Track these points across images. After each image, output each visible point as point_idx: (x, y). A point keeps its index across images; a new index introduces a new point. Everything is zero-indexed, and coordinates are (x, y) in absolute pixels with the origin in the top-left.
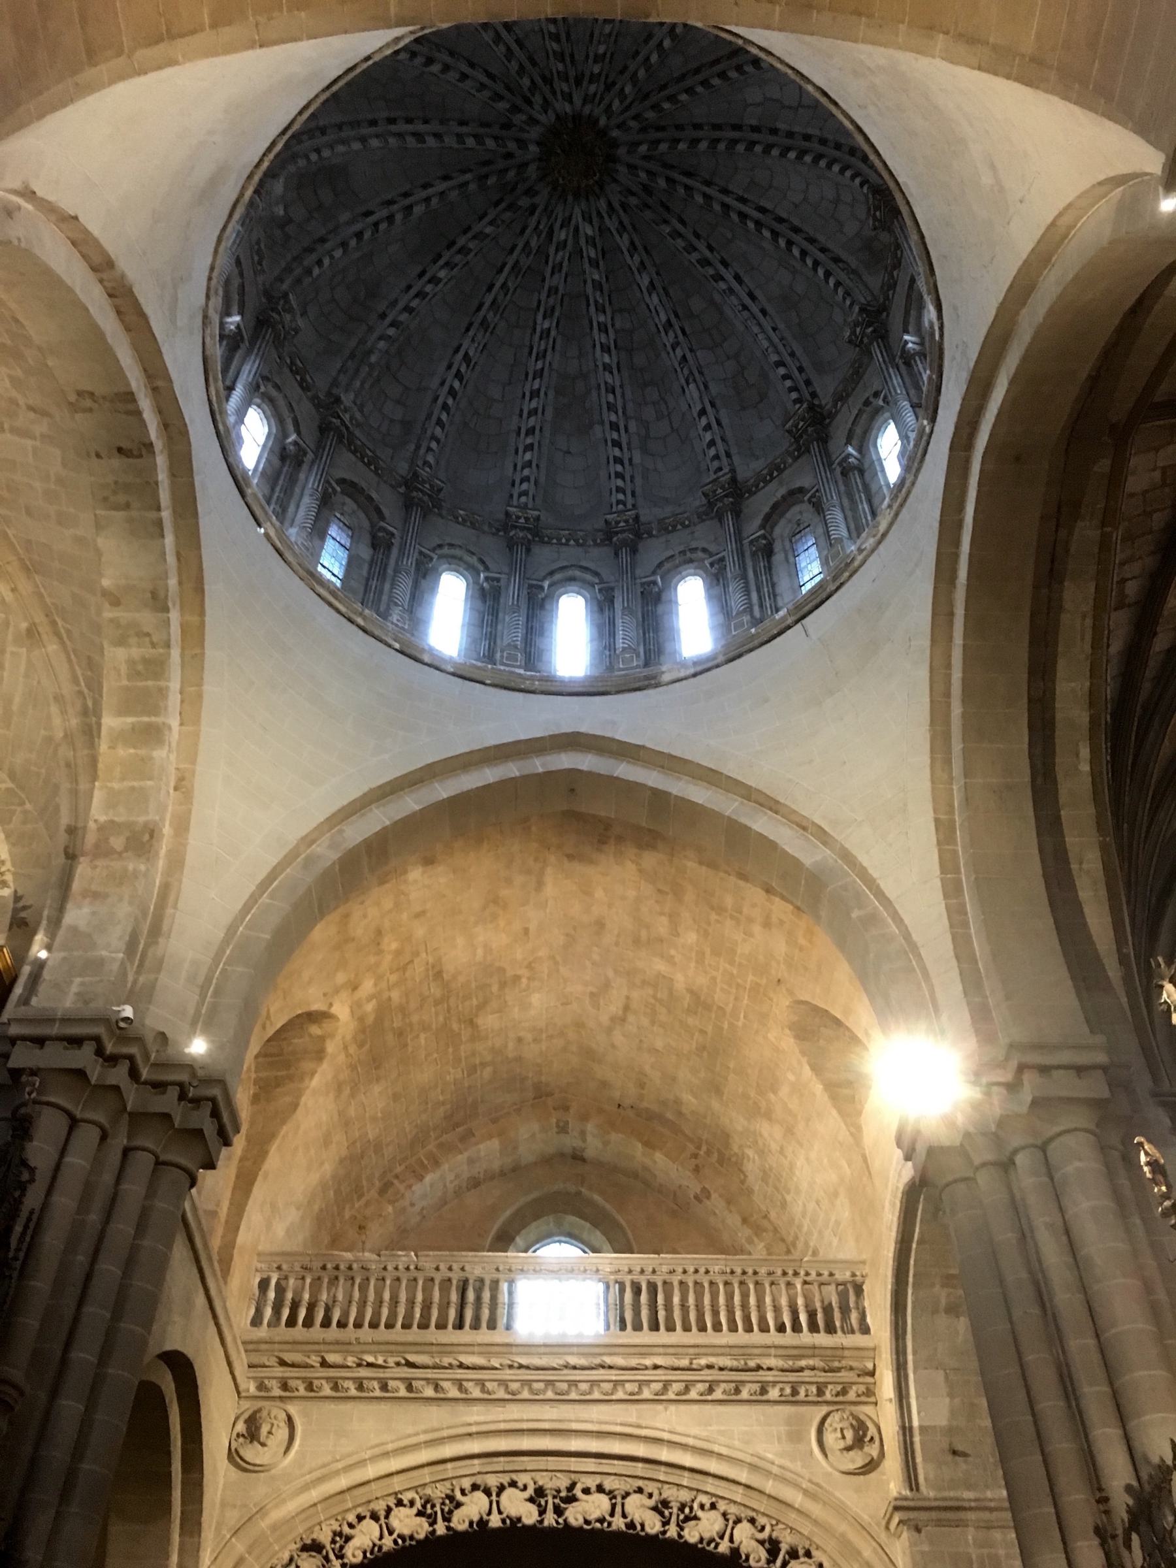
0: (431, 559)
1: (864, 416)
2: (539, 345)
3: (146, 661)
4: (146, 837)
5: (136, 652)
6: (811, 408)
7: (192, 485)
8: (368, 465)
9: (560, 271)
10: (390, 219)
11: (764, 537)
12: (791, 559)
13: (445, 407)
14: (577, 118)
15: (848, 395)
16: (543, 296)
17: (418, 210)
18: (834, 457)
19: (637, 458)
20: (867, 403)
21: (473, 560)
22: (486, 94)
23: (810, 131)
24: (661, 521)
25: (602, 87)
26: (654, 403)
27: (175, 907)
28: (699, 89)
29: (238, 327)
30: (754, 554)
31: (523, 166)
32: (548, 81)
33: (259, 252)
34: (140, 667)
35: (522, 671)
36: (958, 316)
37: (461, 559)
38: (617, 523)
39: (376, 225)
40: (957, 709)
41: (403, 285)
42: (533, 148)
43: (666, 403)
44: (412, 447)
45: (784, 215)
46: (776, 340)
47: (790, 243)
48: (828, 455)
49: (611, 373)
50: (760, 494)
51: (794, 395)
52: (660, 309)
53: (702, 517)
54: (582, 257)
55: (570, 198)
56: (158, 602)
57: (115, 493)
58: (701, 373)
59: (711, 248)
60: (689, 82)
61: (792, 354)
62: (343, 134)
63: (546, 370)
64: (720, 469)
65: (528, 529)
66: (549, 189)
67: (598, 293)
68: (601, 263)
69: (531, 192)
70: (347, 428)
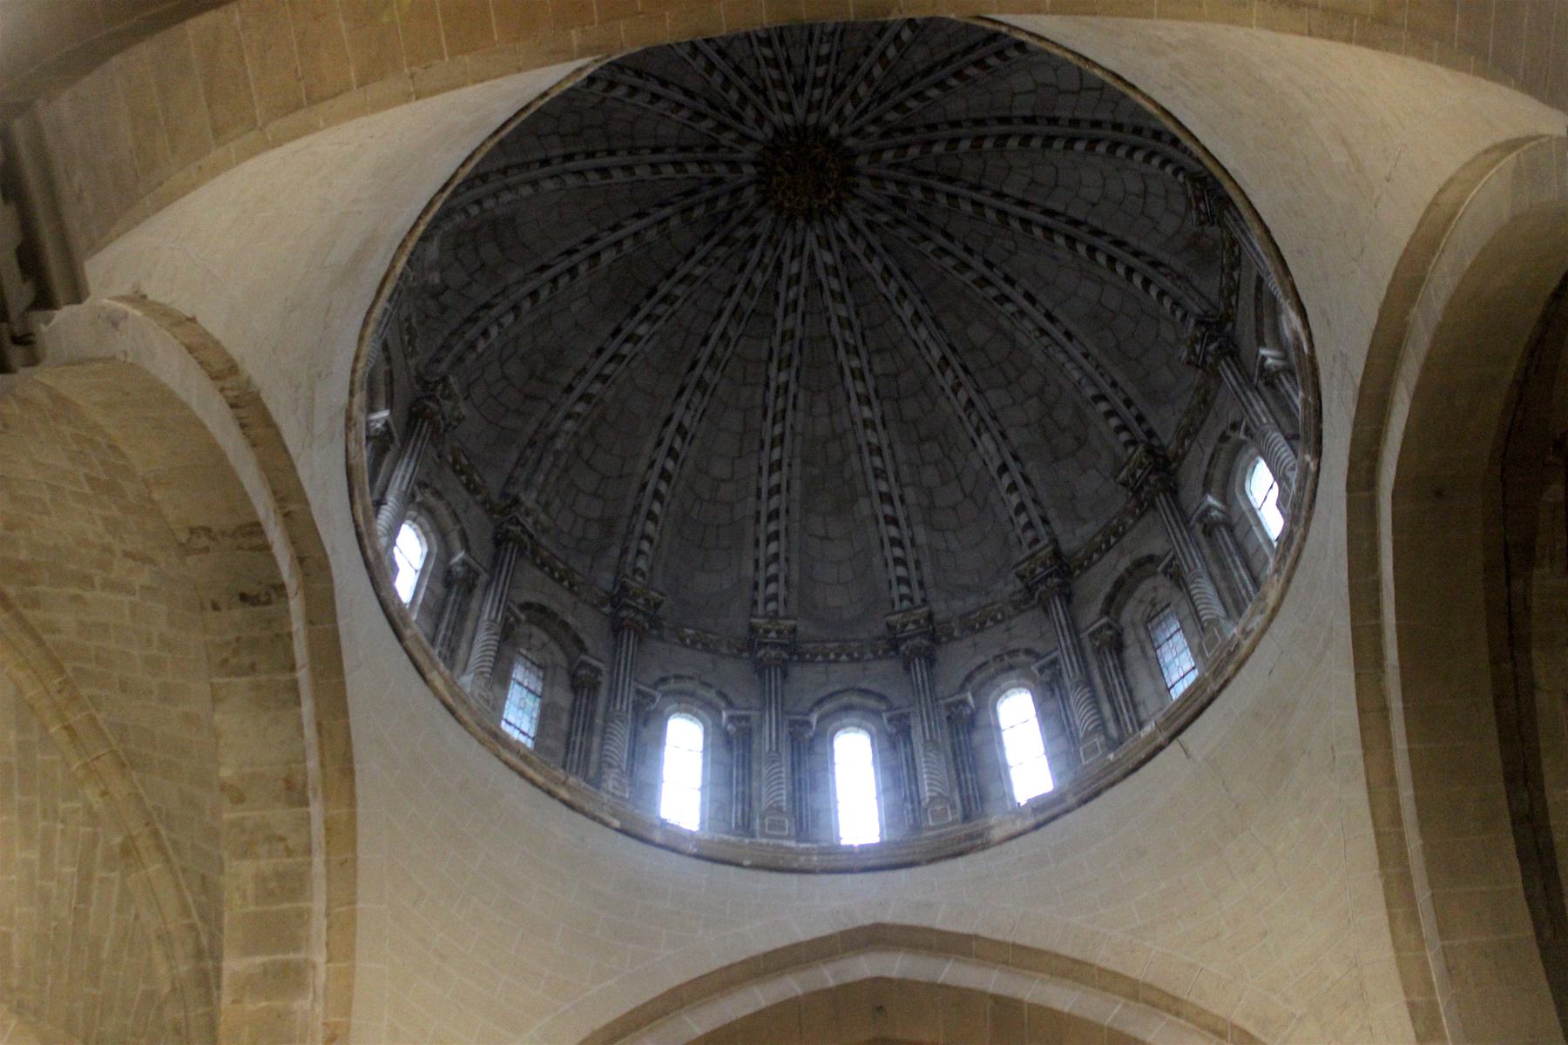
0: (653, 699)
1: (1223, 455)
2: (775, 405)
3: (281, 876)
5: (266, 865)
6: (1150, 451)
7: (336, 630)
8: (561, 580)
9: (795, 310)
10: (572, 271)
11: (1109, 627)
12: (1151, 653)
13: (657, 495)
14: (801, 130)
15: (1197, 432)
16: (776, 340)
17: (607, 257)
18: (1190, 511)
19: (922, 536)
20: (1224, 438)
21: (711, 694)
22: (685, 113)
23: (1099, 116)
24: (964, 617)
25: (829, 91)
28: (953, 82)
29: (386, 424)
30: (1098, 651)
31: (736, 191)
32: (763, 92)
33: (410, 330)
34: (272, 885)
35: (792, 844)
37: (693, 695)
38: (904, 625)
39: (554, 280)
40: (1414, 842)
41: (592, 349)
42: (749, 170)
44: (615, 551)
45: (1081, 216)
46: (1089, 368)
47: (1092, 250)
48: (1182, 512)
49: (875, 430)
50: (1094, 570)
51: (1124, 436)
52: (931, 344)
53: (1020, 606)
54: (822, 291)
55: (800, 224)
56: (294, 792)
57: (236, 652)
58: (995, 418)
60: (940, 74)
61: (1114, 384)
62: (510, 180)
63: (788, 432)
64: (1036, 541)
65: (782, 646)
66: (773, 215)
67: (847, 333)
68: (848, 296)
69: (748, 221)
70: (531, 536)
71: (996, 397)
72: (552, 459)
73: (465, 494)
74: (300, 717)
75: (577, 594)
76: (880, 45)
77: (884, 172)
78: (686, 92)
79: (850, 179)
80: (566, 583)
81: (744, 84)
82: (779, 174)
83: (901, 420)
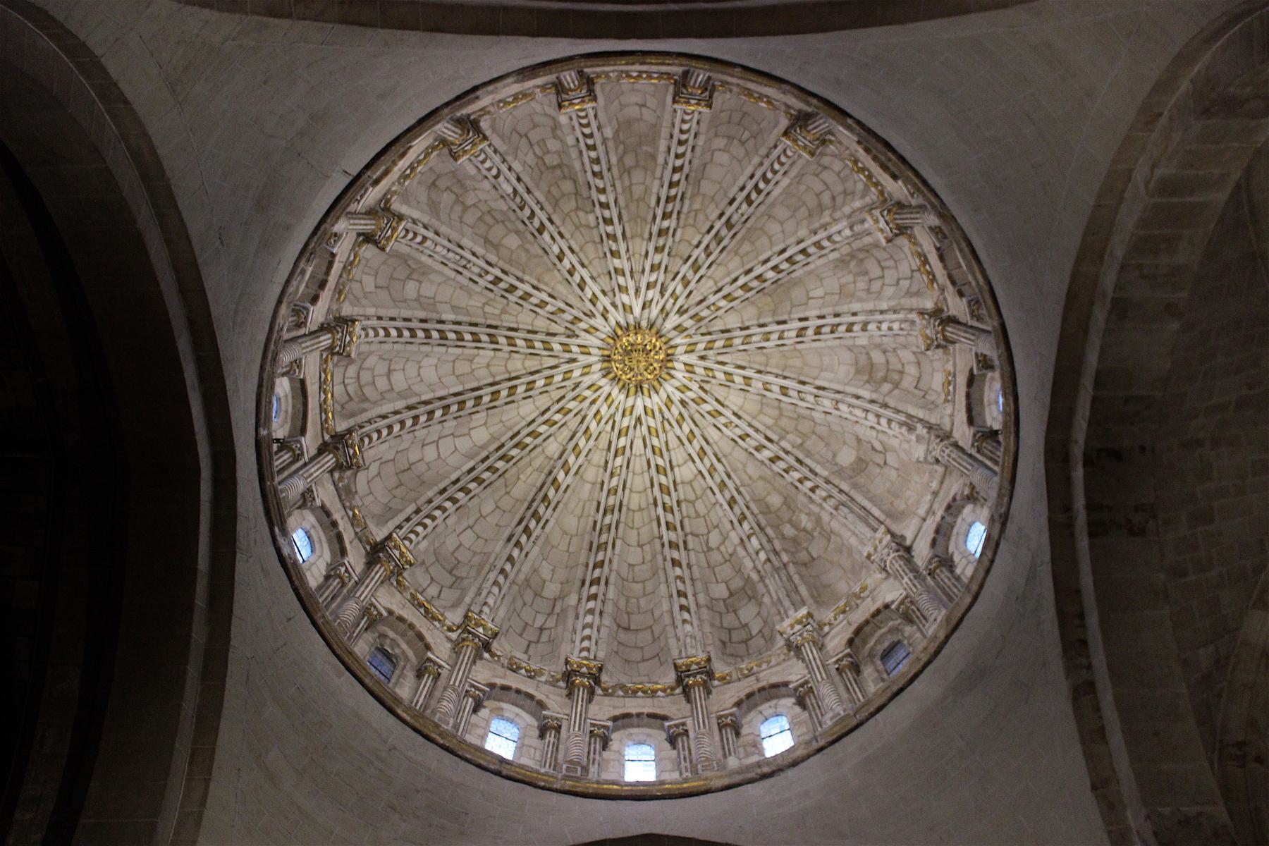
14: (639, 388)
15: (344, 267)
16: (669, 243)
25: (618, 418)
26: (548, 152)
39: (832, 332)
40: (145, 218)
43: (534, 153)
52: (551, 242)
66: (664, 332)
68: (613, 271)
72: (855, 228)
73: (929, 256)
75: (852, 155)
76: (580, 461)
77: (581, 357)
78: (719, 429)
79: (606, 353)
80: (860, 165)
81: (678, 432)
83: (575, 182)
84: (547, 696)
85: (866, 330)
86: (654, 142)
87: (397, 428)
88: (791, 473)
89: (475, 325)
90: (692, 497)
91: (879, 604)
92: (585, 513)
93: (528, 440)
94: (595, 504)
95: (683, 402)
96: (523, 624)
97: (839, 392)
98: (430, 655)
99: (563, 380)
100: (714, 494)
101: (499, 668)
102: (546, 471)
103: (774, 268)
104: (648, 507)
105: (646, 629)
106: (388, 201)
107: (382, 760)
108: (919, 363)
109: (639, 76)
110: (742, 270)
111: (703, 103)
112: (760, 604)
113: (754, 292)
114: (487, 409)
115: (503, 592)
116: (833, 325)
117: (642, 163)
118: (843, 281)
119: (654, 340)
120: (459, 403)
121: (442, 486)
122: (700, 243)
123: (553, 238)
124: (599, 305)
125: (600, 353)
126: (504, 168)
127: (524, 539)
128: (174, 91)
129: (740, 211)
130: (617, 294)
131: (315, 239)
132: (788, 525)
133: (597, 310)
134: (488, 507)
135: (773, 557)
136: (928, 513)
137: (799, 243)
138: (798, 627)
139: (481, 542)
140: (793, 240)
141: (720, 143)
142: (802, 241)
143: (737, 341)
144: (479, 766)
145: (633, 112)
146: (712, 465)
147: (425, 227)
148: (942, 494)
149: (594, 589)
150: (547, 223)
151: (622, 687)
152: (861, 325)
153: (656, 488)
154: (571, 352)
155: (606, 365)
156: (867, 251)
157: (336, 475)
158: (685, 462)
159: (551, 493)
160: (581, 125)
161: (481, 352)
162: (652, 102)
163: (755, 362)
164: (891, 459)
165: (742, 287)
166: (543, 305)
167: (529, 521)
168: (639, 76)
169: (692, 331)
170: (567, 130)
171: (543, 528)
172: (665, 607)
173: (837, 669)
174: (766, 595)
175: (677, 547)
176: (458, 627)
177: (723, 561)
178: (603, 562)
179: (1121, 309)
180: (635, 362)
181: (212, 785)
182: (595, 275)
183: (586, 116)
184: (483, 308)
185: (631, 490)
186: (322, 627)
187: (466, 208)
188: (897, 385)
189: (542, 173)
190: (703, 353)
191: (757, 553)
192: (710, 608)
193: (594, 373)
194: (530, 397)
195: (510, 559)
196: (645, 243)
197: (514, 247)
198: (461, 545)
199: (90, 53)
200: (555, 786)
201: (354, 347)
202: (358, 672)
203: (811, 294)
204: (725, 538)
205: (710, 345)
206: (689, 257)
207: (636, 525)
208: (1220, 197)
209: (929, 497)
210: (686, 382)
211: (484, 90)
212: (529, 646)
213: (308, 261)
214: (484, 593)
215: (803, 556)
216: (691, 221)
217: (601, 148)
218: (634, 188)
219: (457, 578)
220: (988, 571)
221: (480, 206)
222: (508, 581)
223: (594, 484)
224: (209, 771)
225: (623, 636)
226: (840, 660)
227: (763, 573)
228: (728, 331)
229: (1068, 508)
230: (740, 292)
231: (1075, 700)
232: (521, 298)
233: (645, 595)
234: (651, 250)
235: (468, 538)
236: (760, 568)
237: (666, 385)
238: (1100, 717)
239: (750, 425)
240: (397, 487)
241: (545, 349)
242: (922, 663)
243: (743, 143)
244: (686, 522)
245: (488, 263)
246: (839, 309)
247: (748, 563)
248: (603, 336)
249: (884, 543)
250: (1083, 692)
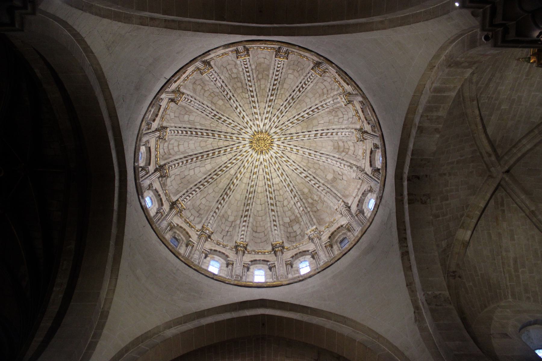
4: (452, 65)
5: (435, 114)
14: (262, 152)
15: (164, 110)
16: (273, 104)
25: (254, 162)
27: (449, 39)
36: (135, 210)
39: (326, 135)
40: (98, 91)
43: (229, 73)
52: (233, 103)
55: (264, 131)
59: (217, 121)
68: (254, 113)
71: (217, 90)
72: (334, 101)
74: (413, 147)
75: (334, 77)
76: (241, 176)
77: (243, 142)
78: (288, 166)
79: (251, 140)
80: (337, 80)
82: (268, 143)
83: (242, 83)
84: (229, 254)
85: (337, 135)
86: (268, 70)
87: (181, 164)
88: (311, 181)
89: (207, 130)
90: (278, 189)
91: (339, 225)
92: (243, 193)
93: (224, 169)
94: (246, 190)
95: (276, 157)
96: (221, 230)
97: (328, 155)
98: (190, 239)
99: (237, 149)
100: (286, 188)
101: (213, 244)
102: (230, 179)
103: (307, 113)
104: (264, 192)
105: (262, 232)
106: (179, 88)
107: (174, 274)
108: (354, 146)
109: (264, 48)
110: (297, 114)
111: (285, 58)
112: (300, 224)
113: (301, 121)
114: (211, 158)
115: (215, 219)
116: (327, 133)
117: (264, 77)
118: (330, 118)
119: (267, 136)
120: (202, 156)
121: (195, 183)
122: (283, 104)
123: (234, 102)
124: (249, 124)
125: (249, 140)
126: (218, 78)
127: (222, 202)
128: (109, 49)
129: (296, 94)
130: (255, 120)
131: (155, 100)
132: (310, 199)
133: (248, 126)
134: (210, 191)
135: (305, 209)
136: (356, 195)
137: (316, 105)
138: (312, 232)
139: (208, 202)
140: (314, 104)
141: (290, 71)
142: (317, 105)
143: (295, 137)
144: (206, 276)
145: (262, 60)
146: (285, 178)
147: (191, 97)
148: (360, 190)
149: (245, 219)
150: (232, 97)
151: (254, 251)
152: (336, 133)
153: (267, 186)
154: (239, 140)
155: (251, 144)
156: (338, 109)
157: (160, 179)
158: (276, 177)
159: (232, 186)
160: (244, 64)
161: (209, 139)
162: (268, 57)
163: (300, 144)
164: (344, 177)
165: (296, 119)
166: (230, 124)
167: (224, 196)
168: (264, 48)
169: (280, 134)
170: (239, 66)
171: (229, 198)
172: (269, 225)
173: (325, 246)
174: (302, 222)
175: (273, 205)
176: (200, 230)
177: (288, 210)
178: (248, 210)
179: (421, 130)
180: (260, 143)
181: (118, 280)
182: (248, 114)
183: (246, 61)
184: (210, 124)
185: (258, 186)
186: (155, 229)
187: (205, 91)
188: (347, 153)
189: (231, 80)
190: (283, 141)
191: (300, 208)
192: (284, 226)
193: (247, 147)
194: (225, 154)
195: (218, 208)
196: (265, 104)
197: (221, 104)
198: (201, 203)
199: (80, 36)
200: (231, 283)
201: (167, 137)
202: (167, 244)
203: (319, 122)
204: (289, 202)
205: (286, 138)
206: (279, 109)
207: (260, 198)
208: (453, 94)
209: (356, 190)
210: (277, 150)
211: (212, 51)
212: (223, 237)
213: (152, 107)
214: (209, 219)
215: (315, 209)
216: (280, 97)
217: (251, 72)
218: (261, 86)
219: (200, 214)
220: (375, 215)
221: (210, 90)
222: (217, 216)
223: (246, 184)
224: (117, 276)
225: (255, 234)
226: (327, 243)
227: (301, 214)
228: (291, 134)
229: (402, 194)
230: (296, 121)
231: (402, 257)
232: (223, 121)
233: (262, 221)
234: (267, 106)
235: (204, 201)
236: (300, 212)
237: (271, 151)
238: (410, 263)
239: (298, 165)
240: (180, 184)
241: (231, 139)
242: (353, 245)
243: (298, 72)
244: (276, 197)
245: (212, 110)
246: (328, 128)
247: (297, 211)
248: (250, 135)
249: (342, 205)
250: (405, 255)
